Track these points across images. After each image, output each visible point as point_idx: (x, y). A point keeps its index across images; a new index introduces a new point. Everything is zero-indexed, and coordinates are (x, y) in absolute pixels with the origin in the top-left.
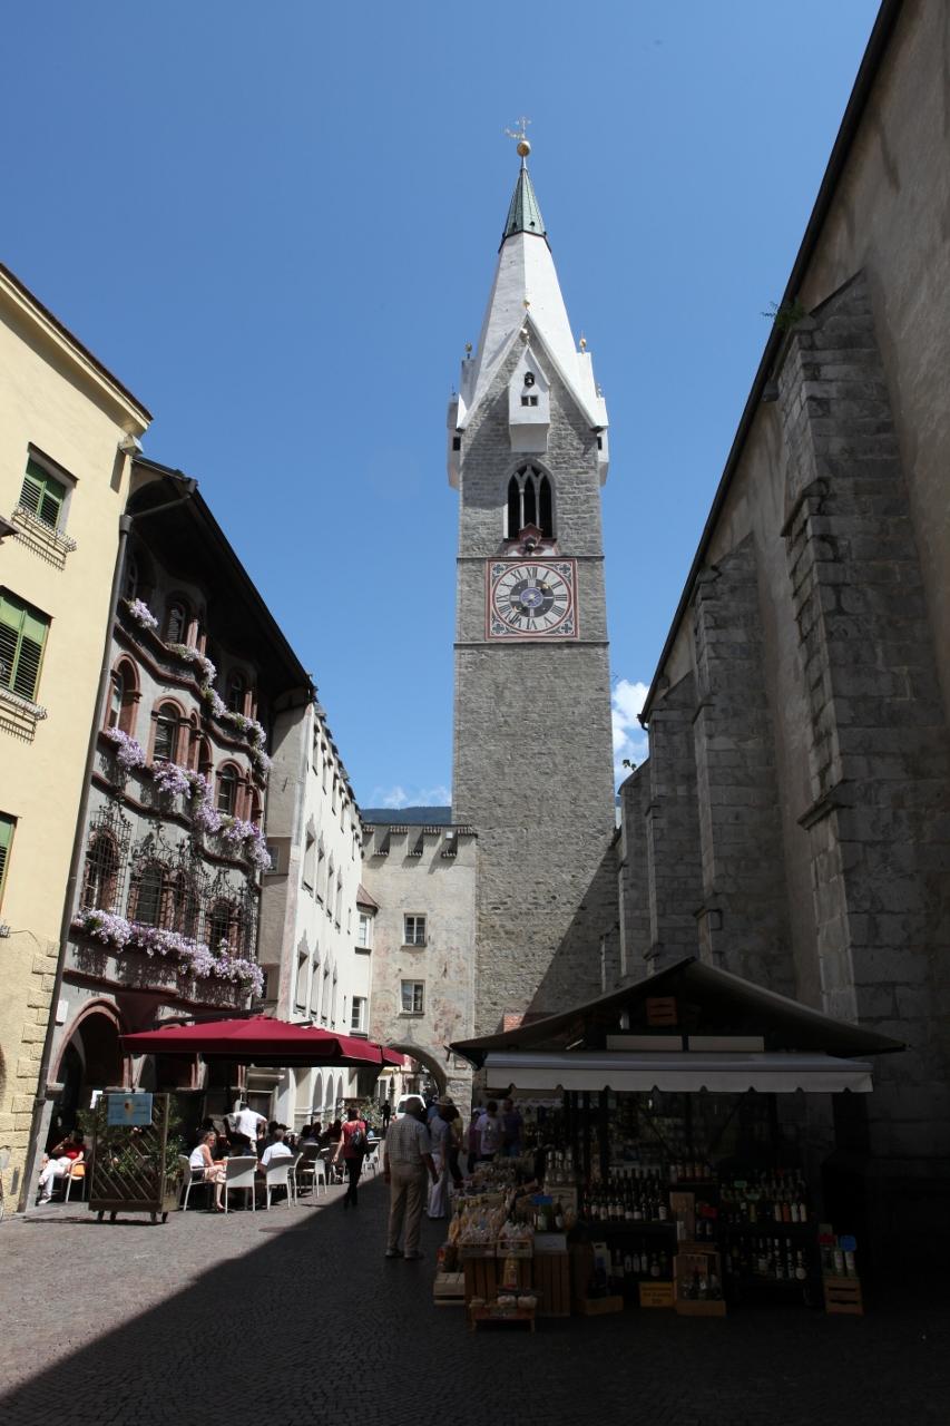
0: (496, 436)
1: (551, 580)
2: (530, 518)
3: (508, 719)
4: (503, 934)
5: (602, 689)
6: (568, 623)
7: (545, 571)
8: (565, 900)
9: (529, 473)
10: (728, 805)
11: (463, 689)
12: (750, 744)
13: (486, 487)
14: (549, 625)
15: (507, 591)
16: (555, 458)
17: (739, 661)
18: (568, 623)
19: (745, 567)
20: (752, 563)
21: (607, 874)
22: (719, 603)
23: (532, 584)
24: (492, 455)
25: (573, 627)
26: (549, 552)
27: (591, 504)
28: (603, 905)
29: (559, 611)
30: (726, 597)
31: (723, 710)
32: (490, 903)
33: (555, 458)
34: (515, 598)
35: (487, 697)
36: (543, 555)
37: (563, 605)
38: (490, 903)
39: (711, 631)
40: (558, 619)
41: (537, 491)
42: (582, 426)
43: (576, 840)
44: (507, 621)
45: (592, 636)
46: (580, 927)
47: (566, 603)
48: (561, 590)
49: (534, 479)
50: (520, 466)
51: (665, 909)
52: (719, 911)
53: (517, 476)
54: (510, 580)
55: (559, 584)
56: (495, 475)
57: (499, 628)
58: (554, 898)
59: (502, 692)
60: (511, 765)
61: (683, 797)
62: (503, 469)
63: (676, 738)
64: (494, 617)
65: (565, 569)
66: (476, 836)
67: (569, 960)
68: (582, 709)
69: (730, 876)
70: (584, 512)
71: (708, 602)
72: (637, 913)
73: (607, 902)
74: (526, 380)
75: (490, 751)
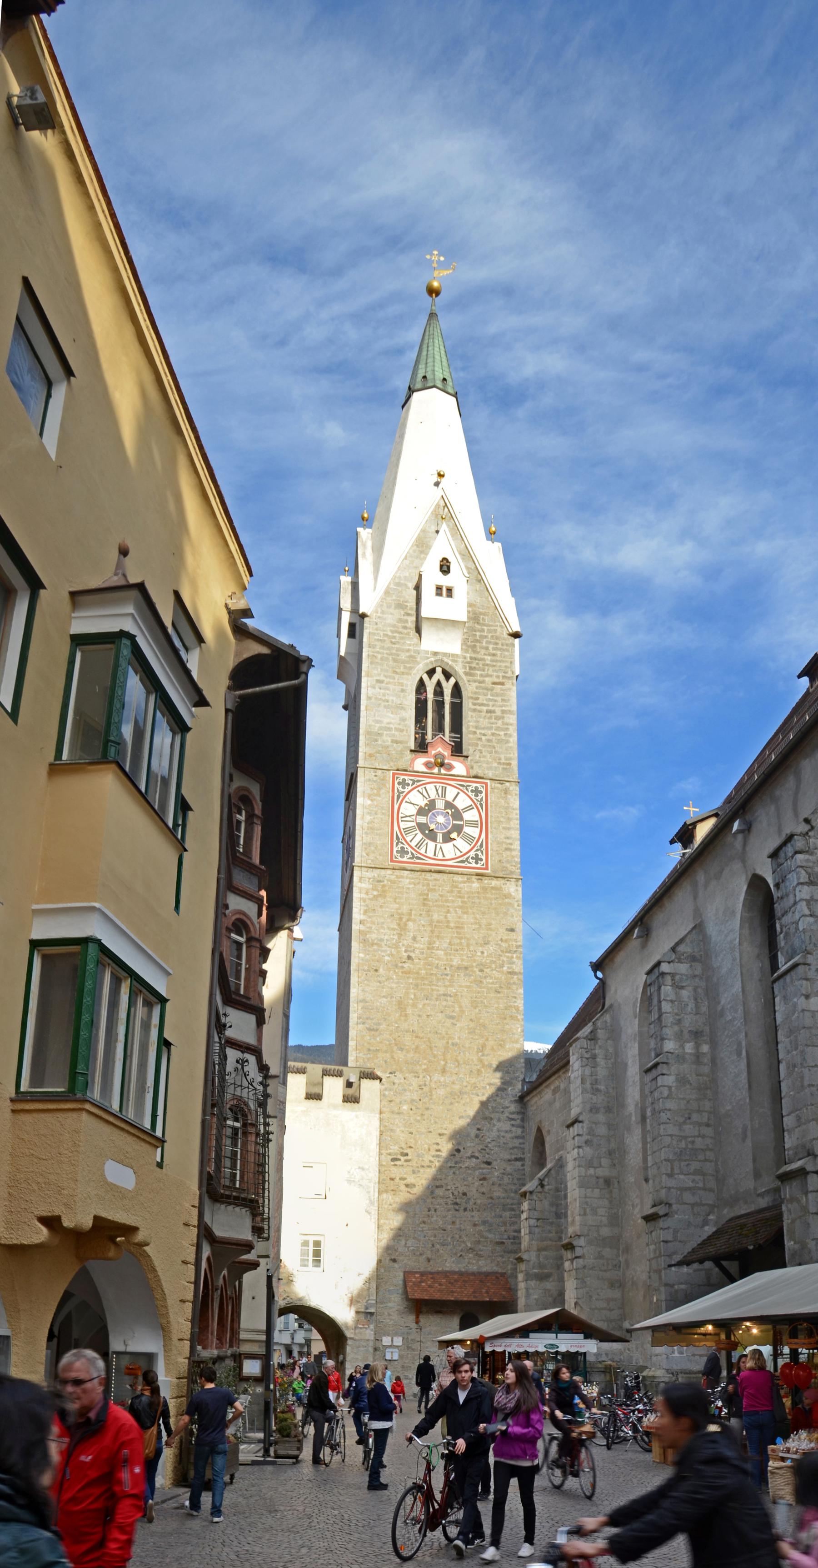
0: (405, 628)
1: (462, 802)
2: (439, 728)
3: (412, 954)
4: (403, 1188)
6: (479, 853)
7: (456, 791)
8: (469, 1154)
9: (439, 675)
11: (362, 917)
13: (391, 687)
14: (459, 854)
15: (413, 810)
16: (468, 663)
18: (479, 853)
21: (514, 1129)
24: (398, 650)
25: (484, 858)
26: (459, 768)
28: (509, 1160)
29: (469, 839)
32: (390, 1154)
34: (422, 819)
35: (389, 928)
36: (453, 772)
37: (474, 832)
38: (390, 1154)
40: (470, 847)
42: (499, 629)
44: (413, 844)
46: (485, 1183)
47: (478, 830)
48: (471, 815)
50: (431, 667)
53: (425, 678)
55: (469, 808)
56: (403, 673)
57: (403, 852)
59: (406, 925)
60: (414, 1005)
62: (411, 668)
65: (477, 792)
67: (473, 1216)
68: (491, 948)
70: (498, 729)
73: (513, 1157)
74: (441, 566)
75: (392, 988)
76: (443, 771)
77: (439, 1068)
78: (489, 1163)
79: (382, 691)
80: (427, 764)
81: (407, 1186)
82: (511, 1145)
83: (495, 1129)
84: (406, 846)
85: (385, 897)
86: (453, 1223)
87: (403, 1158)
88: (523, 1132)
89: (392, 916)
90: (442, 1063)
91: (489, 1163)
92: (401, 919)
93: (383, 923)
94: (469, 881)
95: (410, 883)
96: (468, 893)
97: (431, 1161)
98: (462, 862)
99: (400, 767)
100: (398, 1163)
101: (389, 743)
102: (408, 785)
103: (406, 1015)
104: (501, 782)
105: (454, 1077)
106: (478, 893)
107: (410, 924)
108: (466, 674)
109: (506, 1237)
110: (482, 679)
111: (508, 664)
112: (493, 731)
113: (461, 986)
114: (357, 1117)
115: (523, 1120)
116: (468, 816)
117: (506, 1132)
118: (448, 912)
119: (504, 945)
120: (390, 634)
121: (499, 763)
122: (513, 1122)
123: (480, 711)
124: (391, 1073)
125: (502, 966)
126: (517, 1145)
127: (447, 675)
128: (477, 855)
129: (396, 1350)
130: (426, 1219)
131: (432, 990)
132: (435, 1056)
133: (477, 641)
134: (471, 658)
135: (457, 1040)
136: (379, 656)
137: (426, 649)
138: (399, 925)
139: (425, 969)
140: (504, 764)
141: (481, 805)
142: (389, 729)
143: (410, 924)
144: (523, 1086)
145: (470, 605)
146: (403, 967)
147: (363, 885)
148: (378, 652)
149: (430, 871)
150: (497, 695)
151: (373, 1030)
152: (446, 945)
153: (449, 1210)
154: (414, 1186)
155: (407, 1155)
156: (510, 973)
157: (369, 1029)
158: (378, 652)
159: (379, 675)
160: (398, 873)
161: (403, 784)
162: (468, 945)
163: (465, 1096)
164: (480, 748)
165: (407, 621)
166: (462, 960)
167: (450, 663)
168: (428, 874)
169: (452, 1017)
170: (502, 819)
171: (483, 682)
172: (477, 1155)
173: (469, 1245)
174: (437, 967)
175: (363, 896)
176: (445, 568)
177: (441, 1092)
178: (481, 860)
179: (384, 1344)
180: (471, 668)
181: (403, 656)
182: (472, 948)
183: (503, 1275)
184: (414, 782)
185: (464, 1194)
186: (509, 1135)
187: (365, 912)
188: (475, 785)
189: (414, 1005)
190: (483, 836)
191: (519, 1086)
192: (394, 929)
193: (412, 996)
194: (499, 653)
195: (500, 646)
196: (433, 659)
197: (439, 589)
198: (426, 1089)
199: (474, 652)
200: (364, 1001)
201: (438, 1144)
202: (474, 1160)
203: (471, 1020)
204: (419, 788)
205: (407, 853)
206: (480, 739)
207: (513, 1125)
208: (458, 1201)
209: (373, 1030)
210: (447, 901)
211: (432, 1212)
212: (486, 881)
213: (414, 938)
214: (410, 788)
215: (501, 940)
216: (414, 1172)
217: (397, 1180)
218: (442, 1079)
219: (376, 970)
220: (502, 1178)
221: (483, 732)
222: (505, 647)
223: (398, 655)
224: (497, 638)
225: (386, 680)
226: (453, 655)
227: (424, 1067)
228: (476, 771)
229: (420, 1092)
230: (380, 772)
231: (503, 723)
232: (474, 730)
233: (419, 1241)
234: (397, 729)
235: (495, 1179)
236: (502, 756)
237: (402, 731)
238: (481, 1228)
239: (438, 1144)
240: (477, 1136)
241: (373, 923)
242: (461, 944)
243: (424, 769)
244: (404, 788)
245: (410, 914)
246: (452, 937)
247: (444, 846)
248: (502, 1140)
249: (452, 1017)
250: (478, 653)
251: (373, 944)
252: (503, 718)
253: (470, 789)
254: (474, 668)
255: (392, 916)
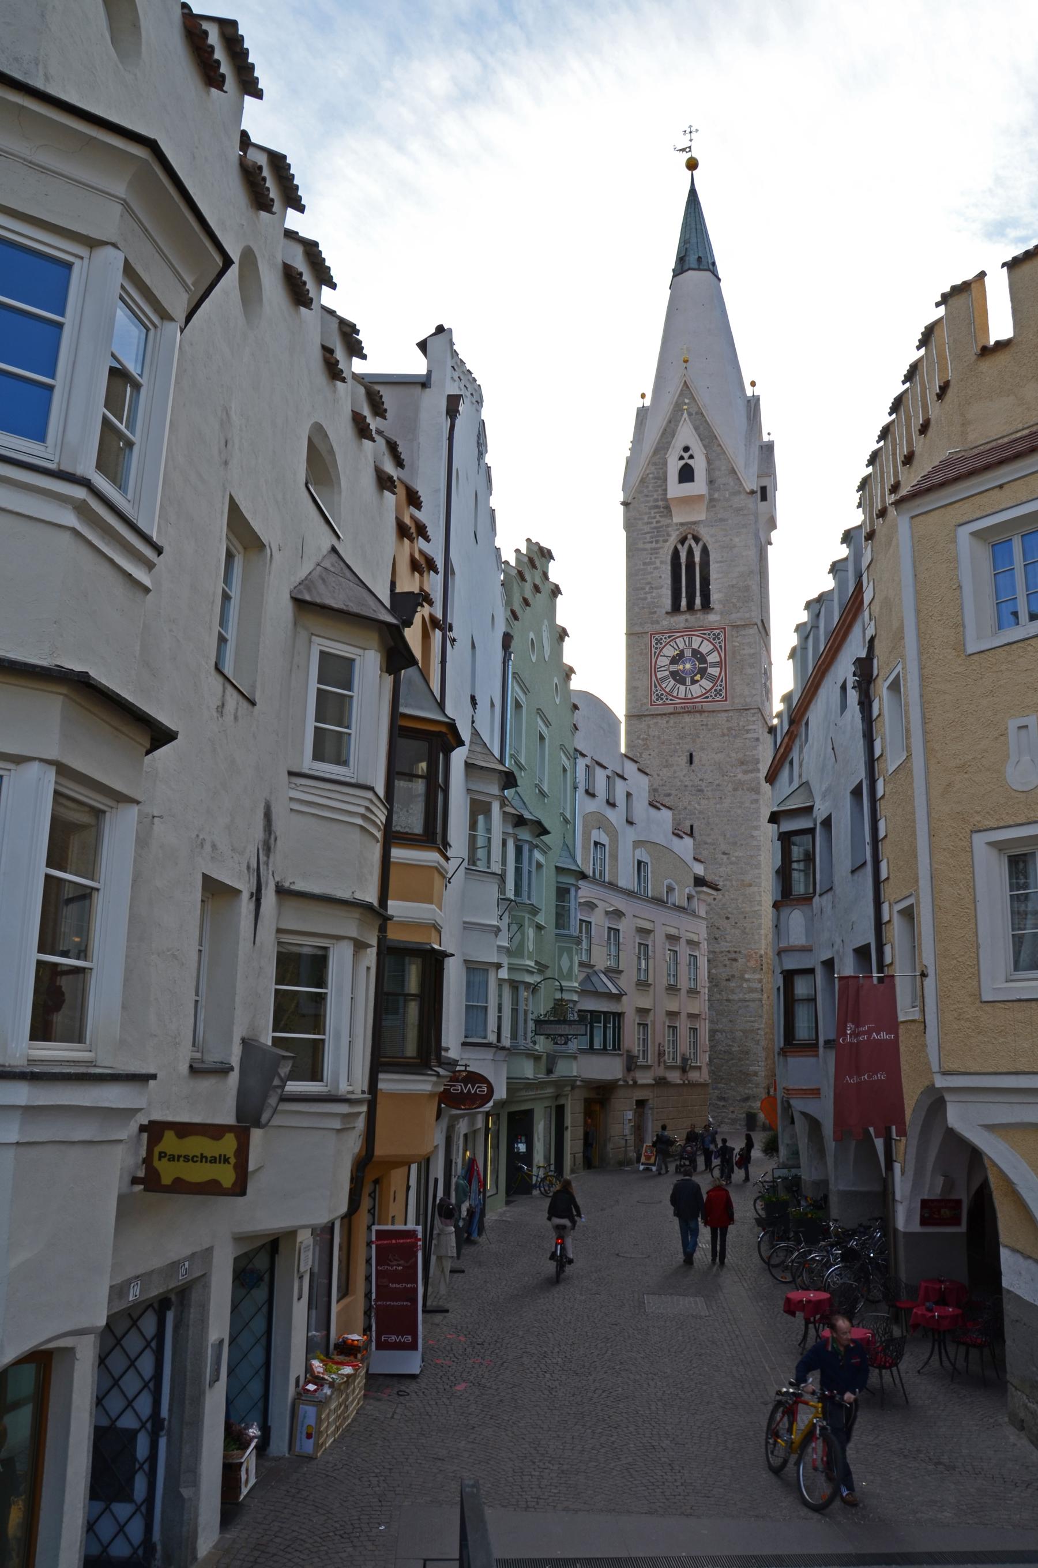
15: (667, 661)
23: (688, 653)
29: (713, 679)
34: (674, 668)
41: (697, 559)
44: (667, 690)
48: (713, 658)
49: (694, 545)
53: (679, 547)
54: (670, 652)
55: (710, 653)
190: (723, 673)
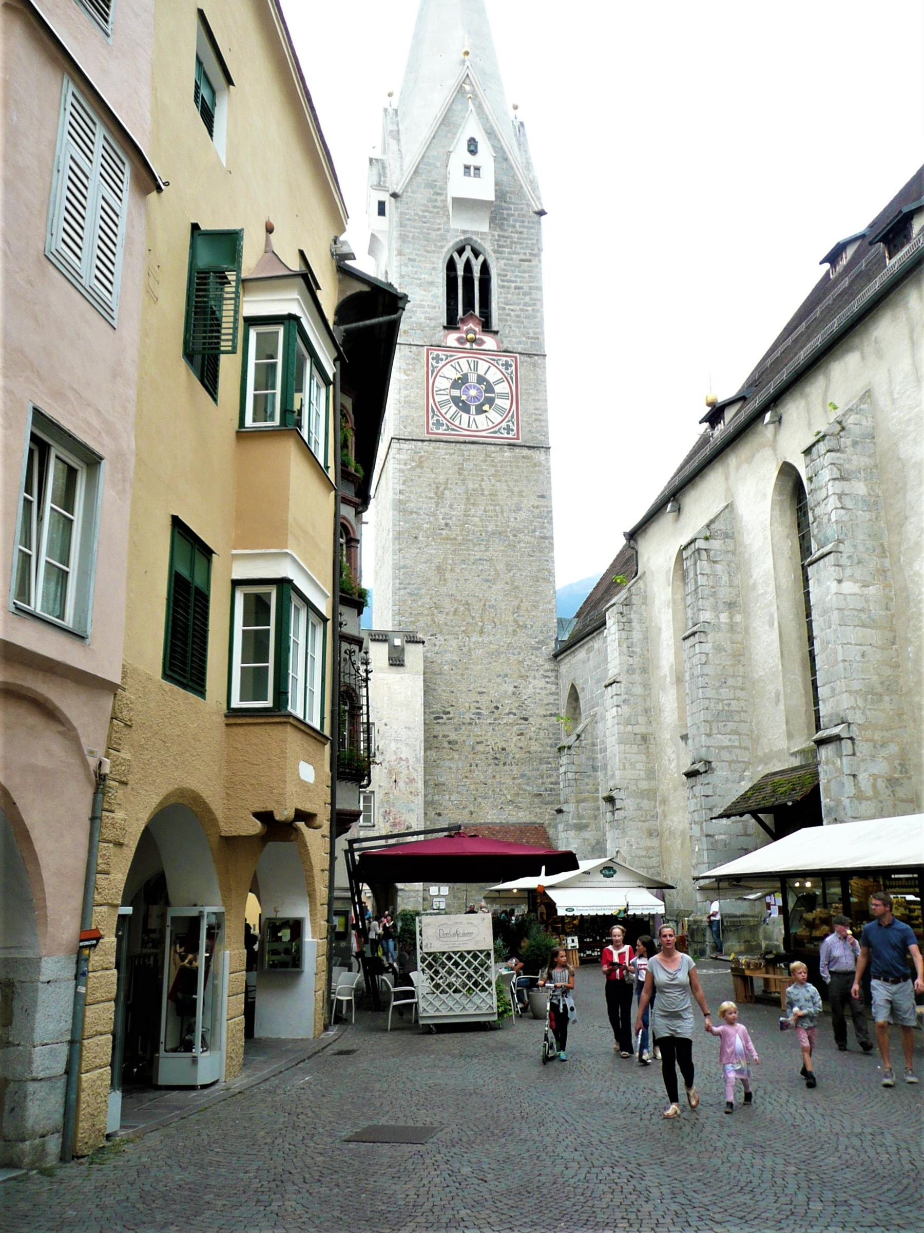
0: (435, 207)
1: (493, 375)
2: (469, 305)
3: (448, 521)
4: (446, 745)
5: (543, 497)
6: (510, 423)
8: (507, 711)
9: (468, 253)
10: (856, 645)
11: (402, 487)
12: (872, 590)
14: (491, 425)
15: (448, 384)
16: (497, 241)
17: (860, 512)
18: (510, 423)
19: (864, 422)
20: (870, 419)
21: (548, 686)
22: (842, 455)
23: (473, 378)
26: (490, 343)
27: (533, 296)
29: (500, 410)
30: (849, 450)
31: (849, 557)
32: (433, 713)
33: (497, 241)
34: (456, 393)
35: (426, 497)
36: (483, 347)
37: (506, 404)
38: (433, 713)
39: (837, 482)
40: (502, 419)
42: (525, 207)
43: (518, 650)
44: (448, 416)
45: (534, 438)
46: (523, 738)
47: (509, 402)
50: (460, 245)
51: (711, 729)
52: (851, 739)
53: (456, 256)
54: (451, 373)
57: (438, 424)
58: (497, 708)
59: (443, 494)
60: (452, 570)
61: (726, 623)
62: (442, 247)
63: (719, 567)
64: (433, 411)
65: (507, 365)
66: (423, 642)
68: (523, 515)
69: (859, 708)
70: (526, 304)
71: (833, 454)
72: (629, 728)
73: (548, 713)
75: (431, 555)
76: (475, 346)
77: (478, 629)
78: (526, 719)
79: (415, 269)
80: (459, 340)
81: (450, 743)
82: (545, 702)
83: (531, 686)
84: (441, 418)
85: (422, 467)
86: (494, 777)
87: (444, 716)
88: (557, 688)
89: (430, 485)
90: (480, 624)
91: (526, 719)
92: (438, 487)
93: (421, 492)
94: (501, 451)
95: (446, 454)
96: (500, 461)
97: (471, 719)
98: (495, 432)
99: (434, 343)
100: (440, 721)
101: (423, 320)
102: (442, 360)
103: (445, 580)
104: (529, 355)
105: (491, 638)
106: (510, 462)
107: (447, 492)
108: (495, 252)
109: (543, 789)
110: (510, 256)
111: (535, 242)
112: (521, 307)
113: (496, 551)
114: (402, 678)
115: (556, 677)
116: (499, 388)
117: (541, 689)
118: (482, 480)
119: (537, 511)
120: (421, 213)
121: (528, 338)
122: (547, 680)
123: (509, 288)
124: (432, 635)
125: (534, 531)
126: (552, 701)
127: (476, 254)
128: (508, 426)
129: (443, 899)
130: (468, 774)
131: (469, 555)
132: (473, 618)
133: (504, 219)
134: (499, 236)
135: (493, 602)
136: (411, 235)
137: (456, 227)
138: (436, 493)
139: (462, 535)
140: (532, 338)
141: (511, 378)
142: (422, 307)
143: (447, 492)
144: (556, 644)
145: (497, 184)
146: (441, 534)
147: (402, 457)
148: (410, 232)
149: (465, 442)
150: (525, 272)
151: (414, 595)
152: (481, 512)
153: (489, 765)
154: (457, 743)
155: (449, 713)
156: (542, 538)
157: (411, 594)
158: (410, 232)
159: (411, 253)
160: (433, 444)
161: (437, 359)
162: (502, 512)
163: (503, 656)
164: (509, 323)
165: (436, 200)
166: (497, 526)
167: (479, 241)
168: (463, 446)
169: (487, 581)
170: (531, 391)
171: (511, 259)
172: (514, 711)
173: (509, 797)
174: (473, 534)
175: (402, 467)
176: (472, 148)
177: (480, 652)
178: (513, 430)
179: (432, 893)
180: (499, 246)
181: (434, 235)
182: (505, 514)
183: (541, 825)
184: (447, 357)
185: (504, 749)
186: (544, 692)
187: (404, 483)
188: (505, 359)
189: (452, 570)
191: (553, 645)
192: (430, 498)
193: (450, 562)
194: (525, 230)
195: (526, 224)
196: (462, 238)
197: (467, 168)
198: (465, 650)
199: (502, 230)
200: (404, 567)
201: (477, 702)
202: (511, 716)
203: (507, 583)
204: (452, 363)
205: (443, 425)
206: (509, 315)
207: (547, 682)
208: (497, 756)
209: (414, 595)
210: (481, 470)
211: (474, 767)
212: (517, 450)
213: (451, 506)
214: (444, 362)
215: (533, 506)
216: (456, 730)
217: (440, 738)
218: (480, 640)
219: (416, 538)
220: (539, 733)
221: (512, 307)
222: (531, 225)
223: (429, 234)
224: (524, 216)
225: (418, 259)
226: (482, 233)
227: (463, 628)
228: (506, 345)
229: (460, 652)
230: (415, 348)
231: (531, 299)
232: (503, 306)
233: (462, 795)
234: (429, 306)
235: (533, 735)
236: (530, 331)
237: (434, 308)
238: (519, 781)
239: (477, 702)
240: (514, 694)
241: (411, 492)
242: (495, 510)
243: (457, 345)
244: (437, 362)
245: (446, 483)
246: (487, 505)
247: (477, 417)
248: (538, 697)
249: (487, 581)
250: (506, 230)
251: (412, 513)
252: (531, 294)
253: (500, 363)
254: (503, 246)
255: (430, 485)
